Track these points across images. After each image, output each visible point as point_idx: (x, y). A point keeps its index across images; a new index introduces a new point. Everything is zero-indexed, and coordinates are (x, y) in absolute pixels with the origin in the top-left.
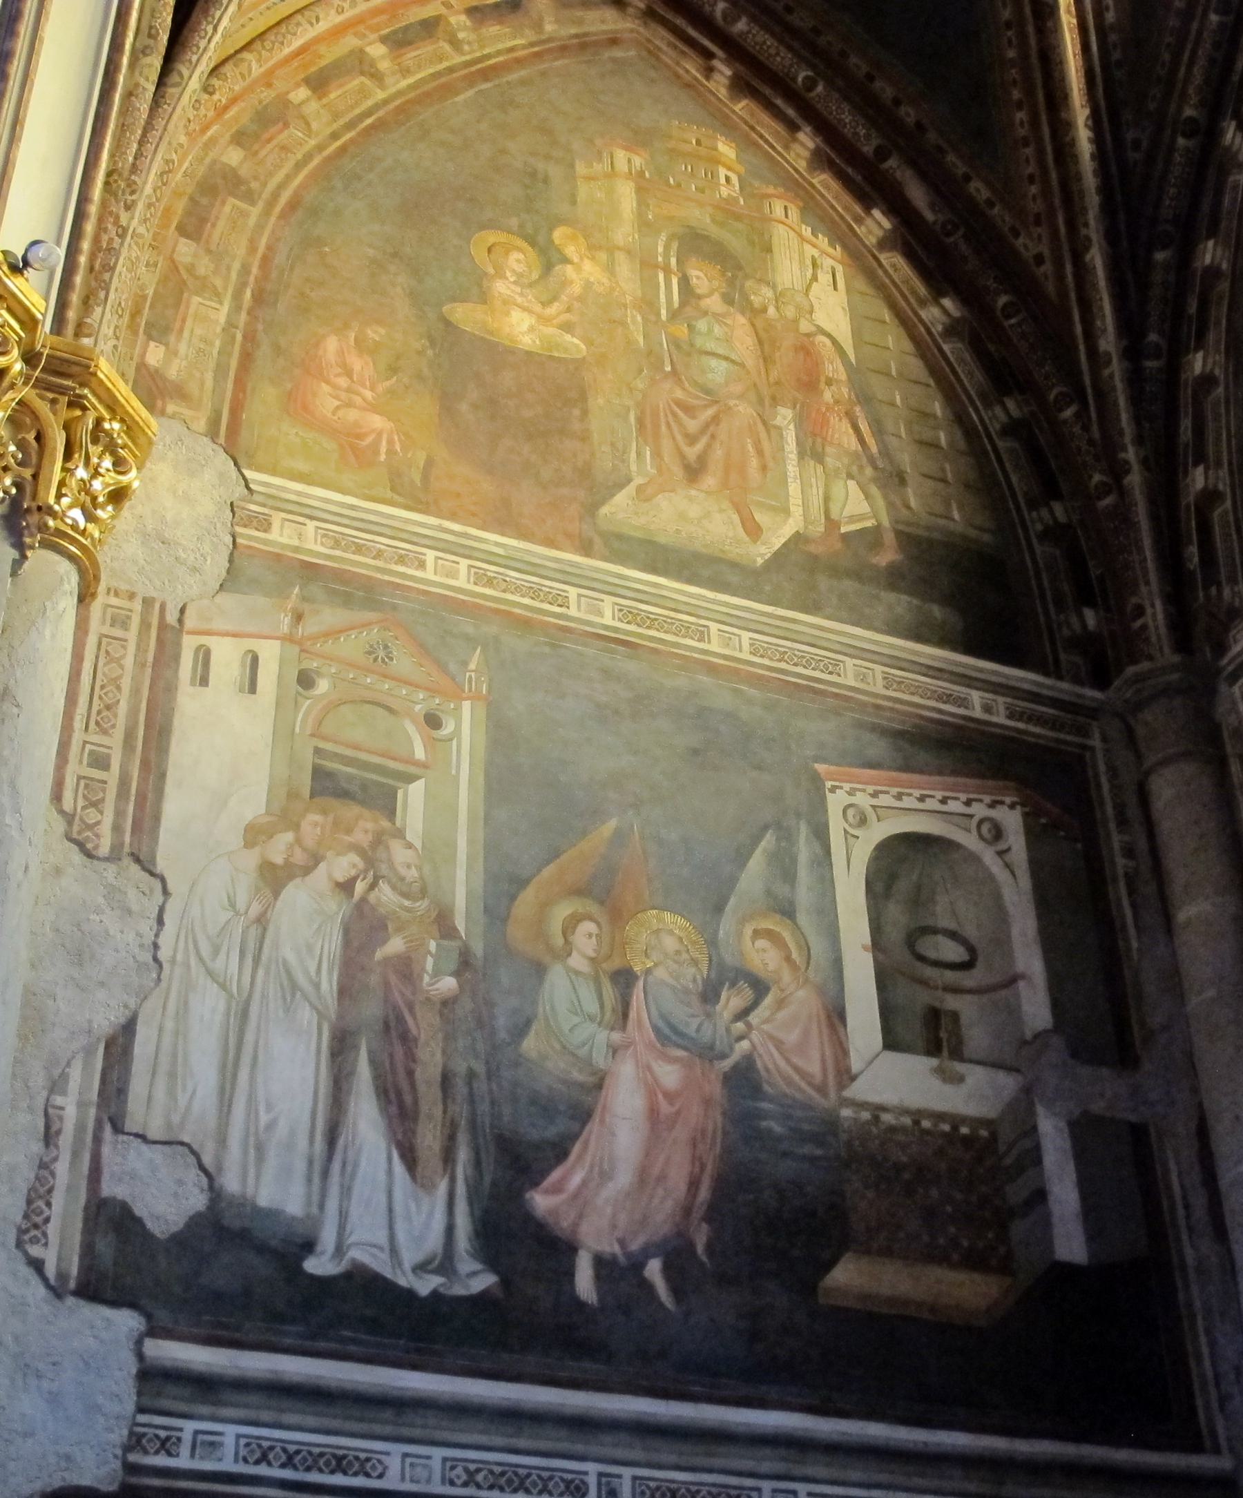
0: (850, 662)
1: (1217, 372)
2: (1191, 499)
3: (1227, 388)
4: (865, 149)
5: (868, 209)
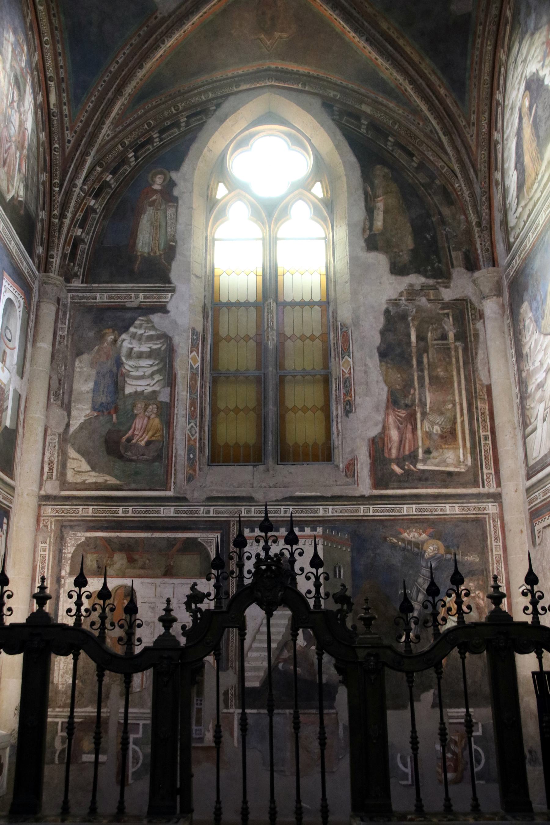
0: (13, 242)
1: (98, 211)
2: (74, 234)
3: (99, 217)
4: (48, 73)
5: (40, 91)
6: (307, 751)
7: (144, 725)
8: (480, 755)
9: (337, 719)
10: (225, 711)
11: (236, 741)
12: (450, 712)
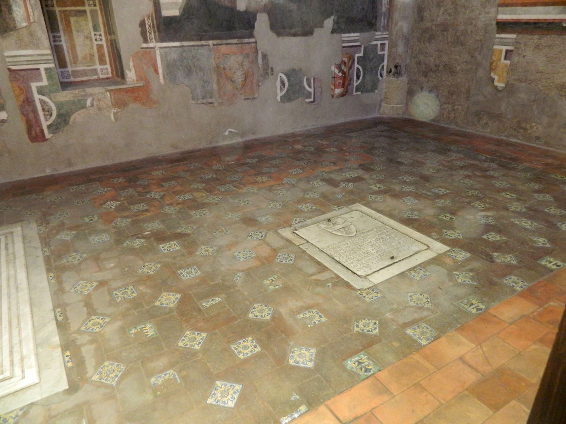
6: (232, 81)
7: (46, 69)
8: (360, 72)
9: (257, 48)
10: (144, 45)
11: (161, 78)
12: (344, 37)
